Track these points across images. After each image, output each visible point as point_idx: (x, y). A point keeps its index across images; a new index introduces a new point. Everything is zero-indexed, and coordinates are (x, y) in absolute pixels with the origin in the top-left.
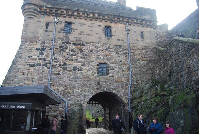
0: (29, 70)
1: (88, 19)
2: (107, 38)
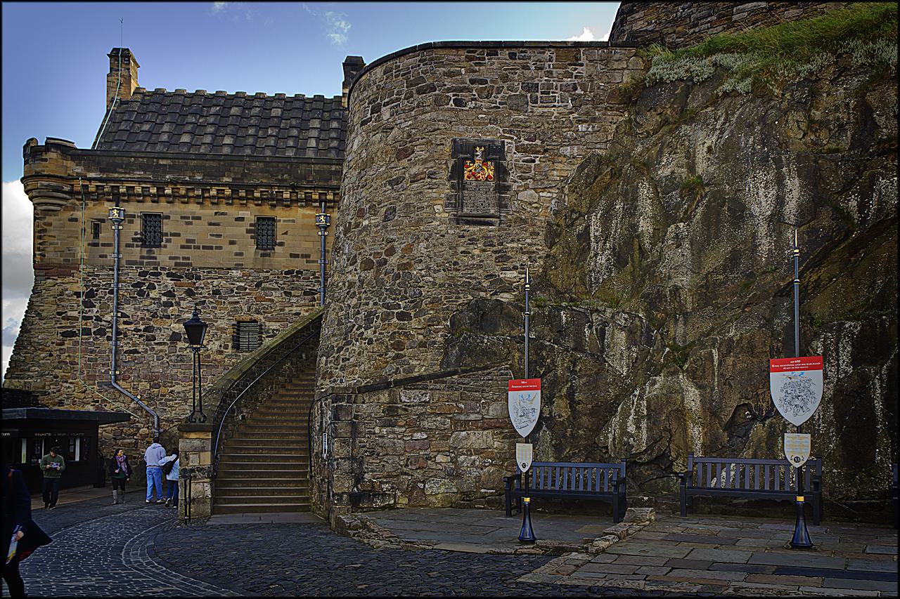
0: (63, 344)
2: (261, 252)
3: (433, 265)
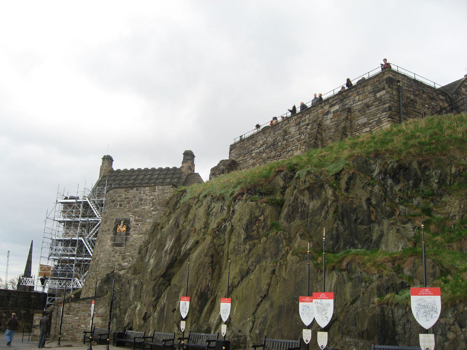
3: (103, 261)
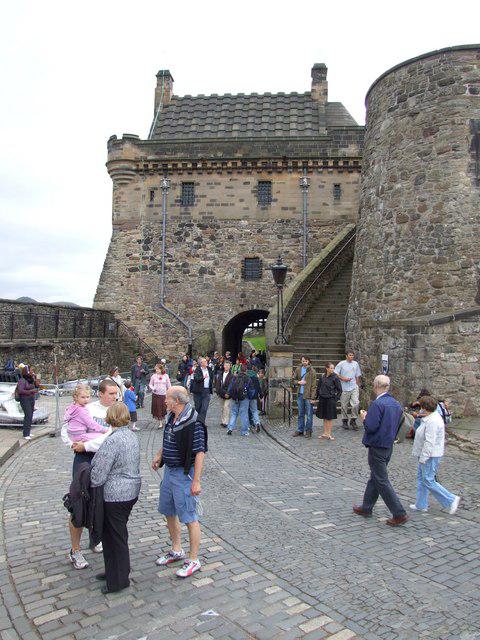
1: (225, 172)
